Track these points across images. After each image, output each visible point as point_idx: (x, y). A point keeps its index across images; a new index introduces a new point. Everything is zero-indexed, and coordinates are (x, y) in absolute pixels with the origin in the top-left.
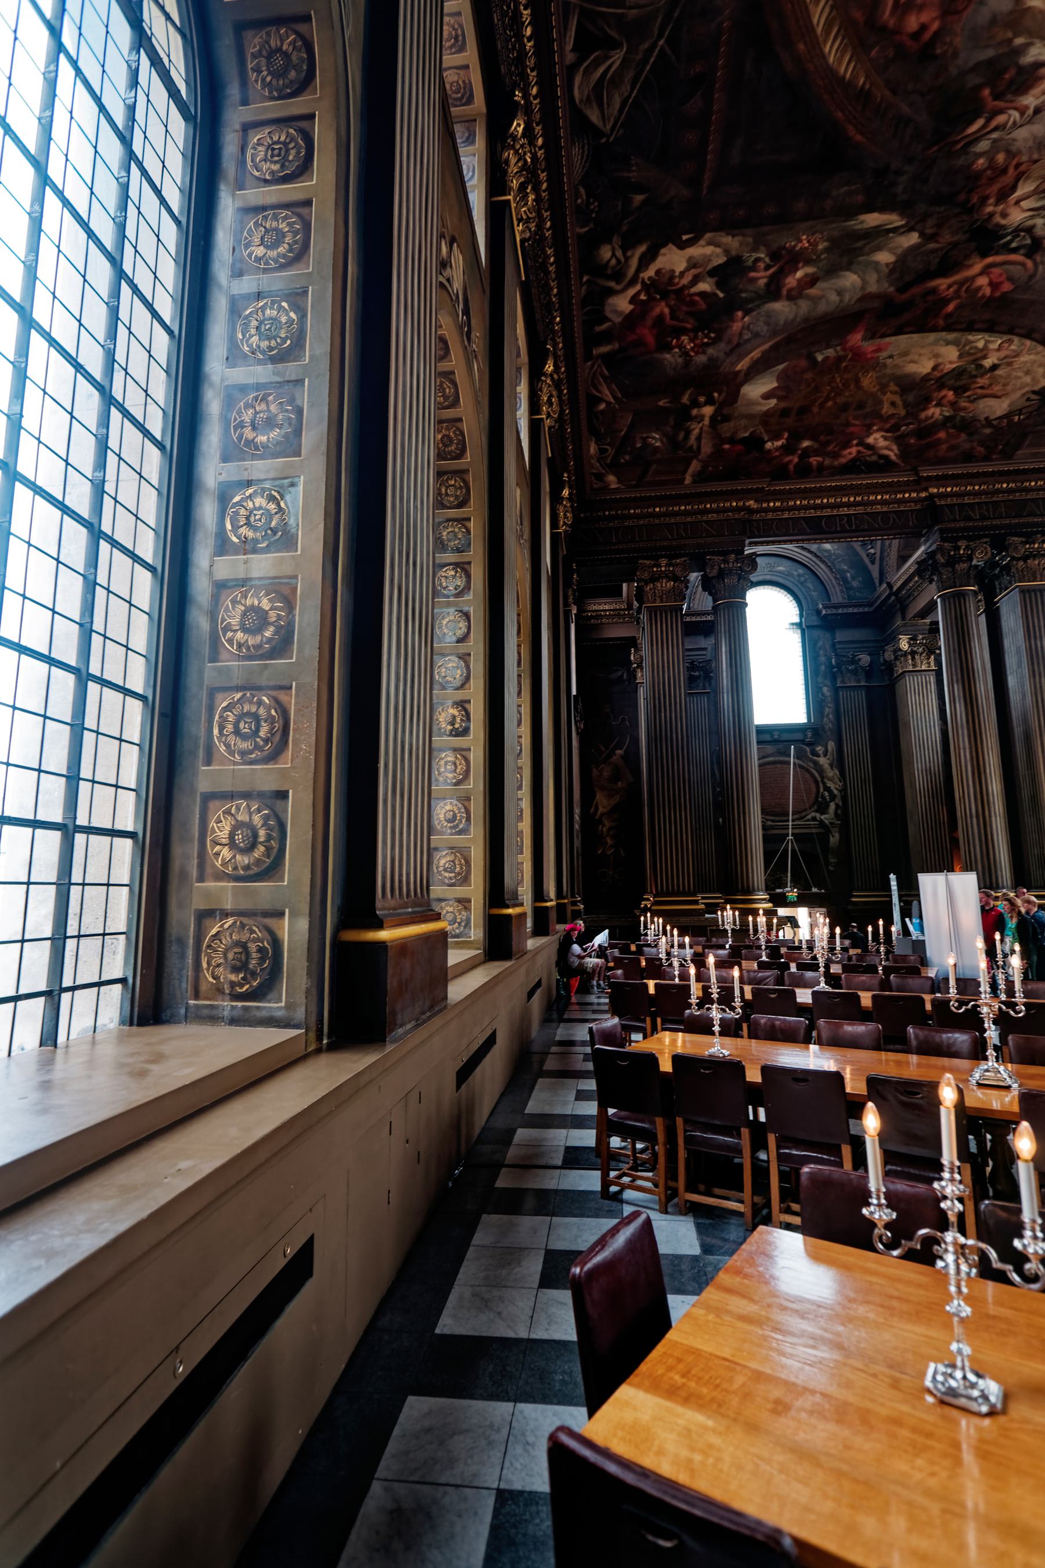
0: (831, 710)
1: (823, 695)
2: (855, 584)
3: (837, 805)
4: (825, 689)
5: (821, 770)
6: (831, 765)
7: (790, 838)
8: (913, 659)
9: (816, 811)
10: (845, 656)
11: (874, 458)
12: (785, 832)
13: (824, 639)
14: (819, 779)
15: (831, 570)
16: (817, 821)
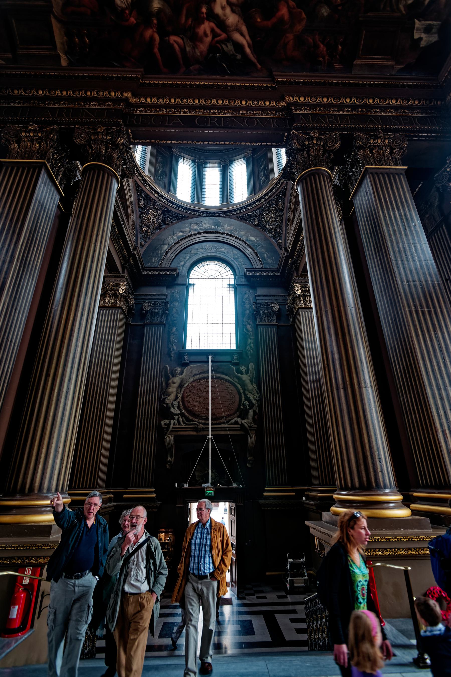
0: (252, 341)
1: (247, 330)
2: (269, 261)
3: (254, 411)
4: (248, 326)
5: (243, 385)
6: (251, 381)
7: (210, 437)
8: (305, 300)
9: (238, 417)
10: (262, 304)
11: (229, 48)
12: (205, 433)
13: (249, 294)
14: (242, 391)
15: (254, 252)
16: (239, 424)
